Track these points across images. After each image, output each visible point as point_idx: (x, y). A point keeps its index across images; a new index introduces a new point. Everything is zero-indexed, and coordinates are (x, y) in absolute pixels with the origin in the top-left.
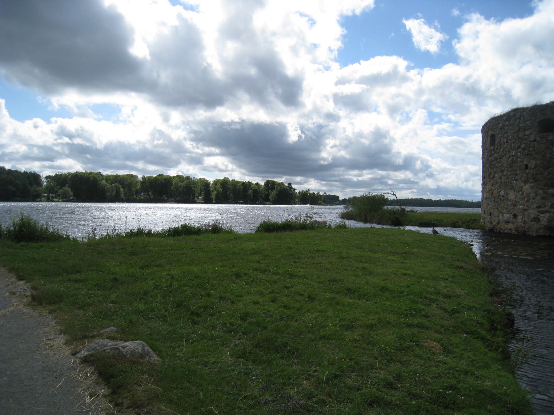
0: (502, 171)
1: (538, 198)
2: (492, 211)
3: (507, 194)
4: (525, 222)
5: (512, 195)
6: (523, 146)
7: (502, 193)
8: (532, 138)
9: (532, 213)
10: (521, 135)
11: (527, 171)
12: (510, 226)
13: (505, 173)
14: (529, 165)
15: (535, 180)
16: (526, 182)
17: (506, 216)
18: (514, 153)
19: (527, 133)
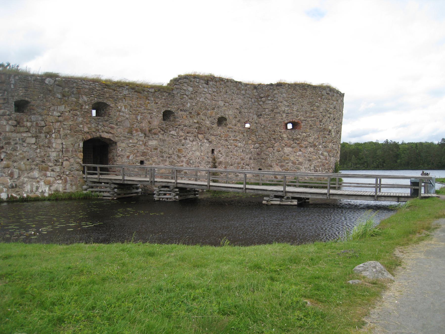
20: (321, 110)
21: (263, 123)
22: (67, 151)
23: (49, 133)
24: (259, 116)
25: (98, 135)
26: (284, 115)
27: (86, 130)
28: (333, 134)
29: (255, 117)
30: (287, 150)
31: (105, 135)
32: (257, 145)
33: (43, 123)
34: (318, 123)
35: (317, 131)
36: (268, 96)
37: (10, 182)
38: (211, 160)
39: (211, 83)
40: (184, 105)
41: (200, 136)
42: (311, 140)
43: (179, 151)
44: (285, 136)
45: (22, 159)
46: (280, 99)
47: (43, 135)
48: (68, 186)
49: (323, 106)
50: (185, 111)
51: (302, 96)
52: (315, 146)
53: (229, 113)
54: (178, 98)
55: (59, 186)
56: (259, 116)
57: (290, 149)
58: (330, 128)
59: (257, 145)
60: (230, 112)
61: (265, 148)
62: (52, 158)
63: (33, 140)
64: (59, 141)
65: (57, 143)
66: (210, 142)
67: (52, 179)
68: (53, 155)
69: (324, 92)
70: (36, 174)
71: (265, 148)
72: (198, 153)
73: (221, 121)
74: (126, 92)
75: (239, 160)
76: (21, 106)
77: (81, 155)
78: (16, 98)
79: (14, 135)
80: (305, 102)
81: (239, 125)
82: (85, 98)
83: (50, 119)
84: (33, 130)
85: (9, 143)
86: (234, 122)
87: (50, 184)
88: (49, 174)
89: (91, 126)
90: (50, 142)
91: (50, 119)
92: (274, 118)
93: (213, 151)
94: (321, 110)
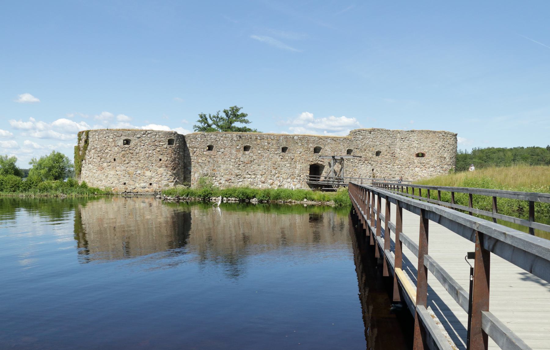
0: (139, 161)
1: (168, 175)
2: (127, 182)
3: (144, 173)
4: (159, 187)
5: (148, 174)
6: (158, 150)
7: (139, 172)
8: (165, 146)
9: (164, 182)
10: (157, 144)
11: (161, 162)
12: (147, 189)
13: (142, 161)
14: (163, 159)
15: (167, 167)
16: (160, 167)
17: (143, 185)
18: (150, 152)
19: (161, 143)
20: (438, 145)
21: (403, 153)
22: (303, 170)
23: (295, 162)
24: (401, 150)
25: (316, 162)
26: (416, 149)
27: (311, 160)
28: (448, 160)
29: (399, 150)
30: (417, 169)
31: (320, 163)
32: (399, 166)
33: (293, 157)
34: (437, 153)
35: (436, 158)
36: (406, 138)
37: (279, 184)
38: (372, 175)
39: (372, 133)
40: (358, 146)
41: (366, 162)
42: (432, 163)
43: (355, 170)
44: (416, 161)
45: (284, 173)
46: (413, 140)
47: (293, 163)
48: (303, 186)
49: (440, 143)
50: (358, 149)
51: (426, 138)
52: (435, 167)
53: (383, 149)
54: (354, 142)
55: (298, 186)
56: (401, 150)
57: (419, 169)
58: (445, 156)
59: (399, 166)
60: (383, 148)
61: (404, 168)
62: (297, 173)
63: (289, 165)
64: (300, 165)
65: (299, 166)
66: (372, 165)
67: (296, 183)
68: (297, 171)
69: (440, 135)
70: (289, 180)
71: (404, 168)
72: (365, 171)
73: (378, 153)
74: (329, 141)
75: (388, 175)
76: (284, 150)
77: (309, 172)
78: (282, 146)
79: (281, 162)
80: (429, 141)
81: (388, 155)
82: (311, 145)
83: (296, 155)
84: (289, 160)
85: (279, 166)
86: (385, 153)
87: (295, 185)
88: (295, 180)
89: (314, 159)
90: (296, 166)
91: (296, 155)
92: (409, 151)
93: (373, 170)
94: (438, 145)
